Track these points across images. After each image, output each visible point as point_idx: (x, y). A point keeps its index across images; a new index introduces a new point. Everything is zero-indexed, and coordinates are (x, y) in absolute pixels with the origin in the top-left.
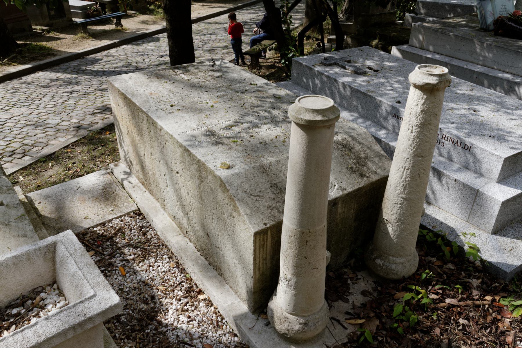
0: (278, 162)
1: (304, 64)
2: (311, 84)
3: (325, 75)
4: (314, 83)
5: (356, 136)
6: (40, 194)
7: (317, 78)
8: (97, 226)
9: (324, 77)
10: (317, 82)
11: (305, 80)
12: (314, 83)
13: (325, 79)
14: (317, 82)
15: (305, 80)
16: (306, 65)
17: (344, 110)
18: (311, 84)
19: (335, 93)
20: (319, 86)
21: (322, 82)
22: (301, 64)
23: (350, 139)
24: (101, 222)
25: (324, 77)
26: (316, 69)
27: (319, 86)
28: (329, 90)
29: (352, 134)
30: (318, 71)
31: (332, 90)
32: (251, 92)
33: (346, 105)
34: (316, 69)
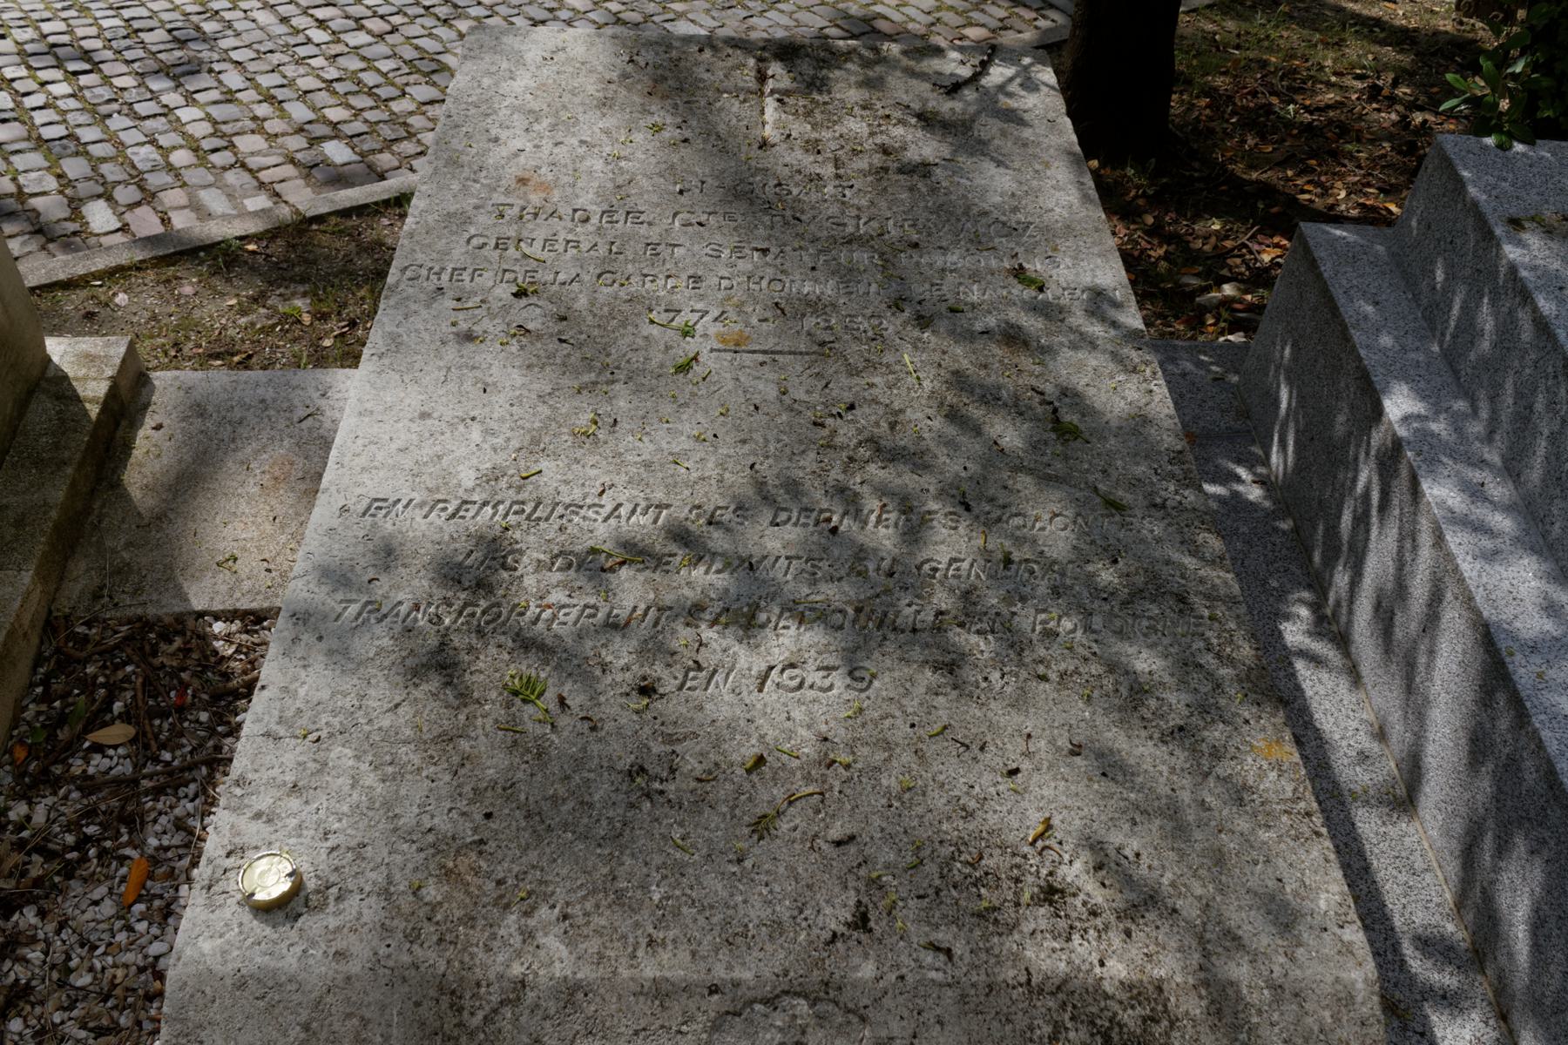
0: (571, 993)
1: (1472, 191)
2: (1456, 311)
3: (1535, 309)
4: (1469, 312)
5: (1259, 996)
6: (188, 390)
7: (1493, 303)
8: (229, 616)
9: (1524, 316)
10: (1487, 321)
11: (1440, 276)
12: (1469, 312)
13: (1527, 333)
14: (1487, 321)
15: (1440, 276)
16: (1475, 204)
17: (1534, 550)
18: (1456, 311)
19: (1536, 433)
20: (1485, 345)
21: (1507, 330)
22: (1460, 184)
23: (1192, 1006)
24: (255, 605)
25: (1524, 316)
26: (1511, 252)
27: (1485, 345)
28: (1519, 395)
29: (1239, 971)
30: (1513, 269)
31: (1530, 407)
32: (969, 336)
33: (1556, 529)
34: (1511, 252)
